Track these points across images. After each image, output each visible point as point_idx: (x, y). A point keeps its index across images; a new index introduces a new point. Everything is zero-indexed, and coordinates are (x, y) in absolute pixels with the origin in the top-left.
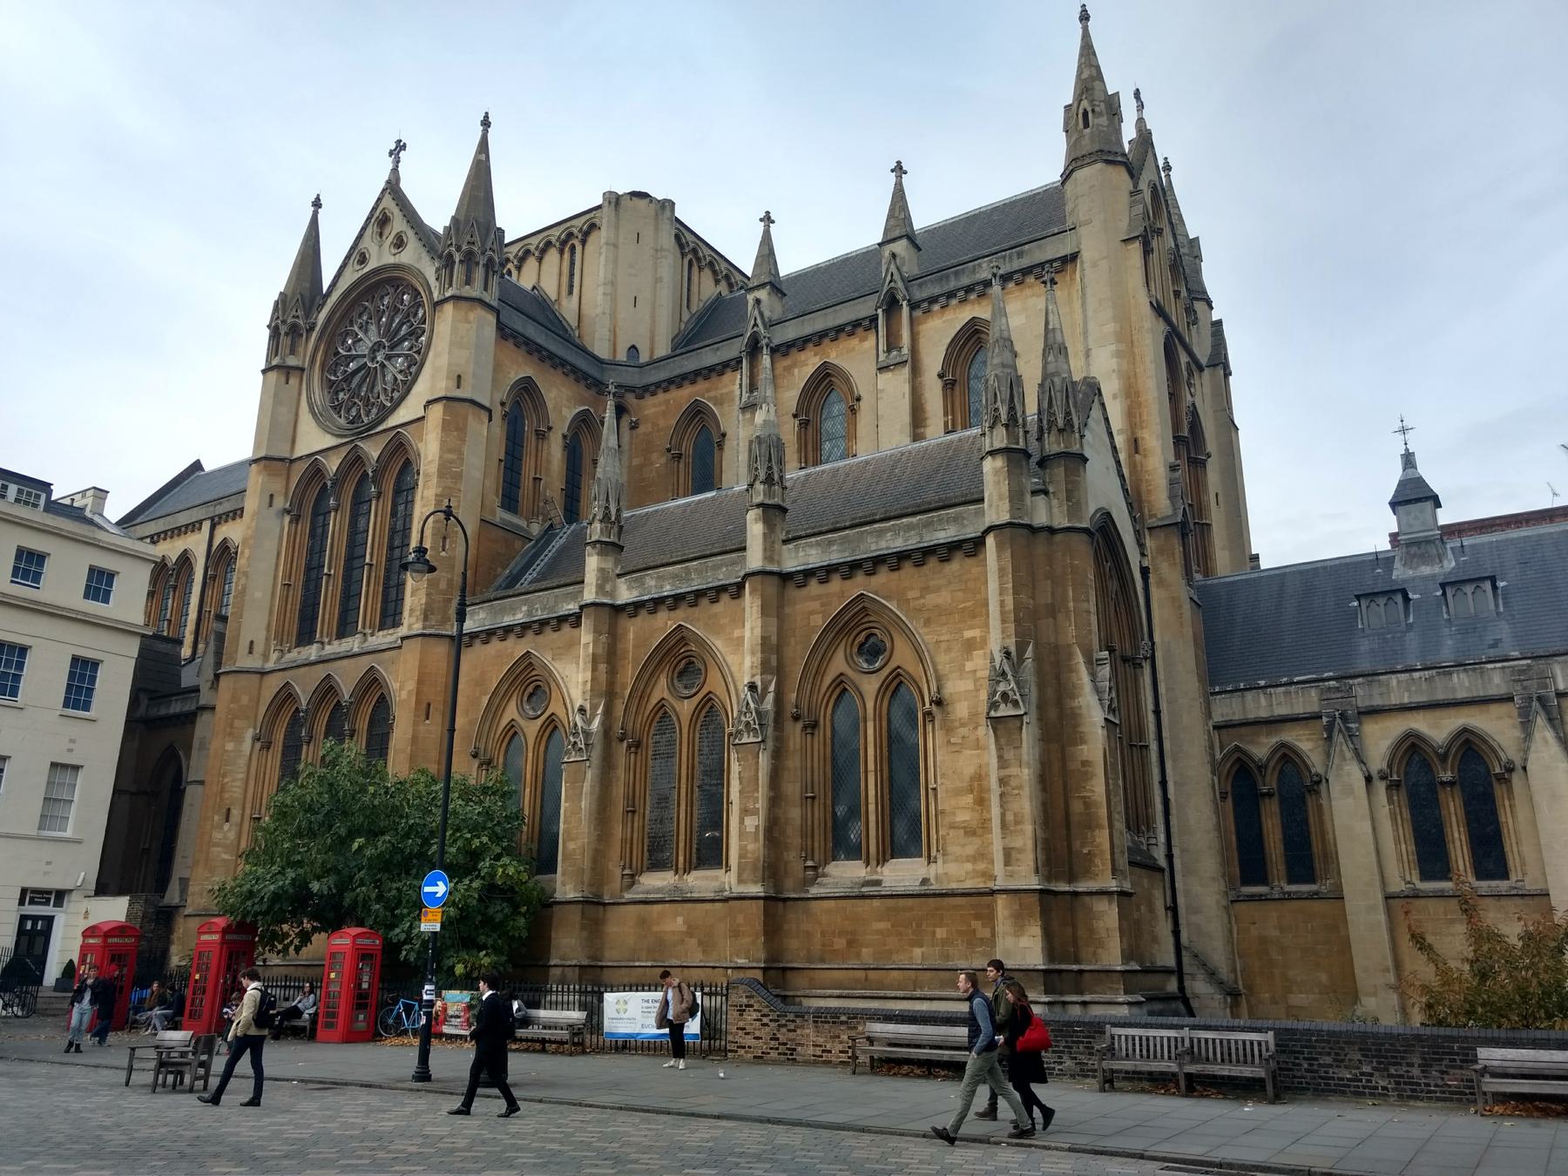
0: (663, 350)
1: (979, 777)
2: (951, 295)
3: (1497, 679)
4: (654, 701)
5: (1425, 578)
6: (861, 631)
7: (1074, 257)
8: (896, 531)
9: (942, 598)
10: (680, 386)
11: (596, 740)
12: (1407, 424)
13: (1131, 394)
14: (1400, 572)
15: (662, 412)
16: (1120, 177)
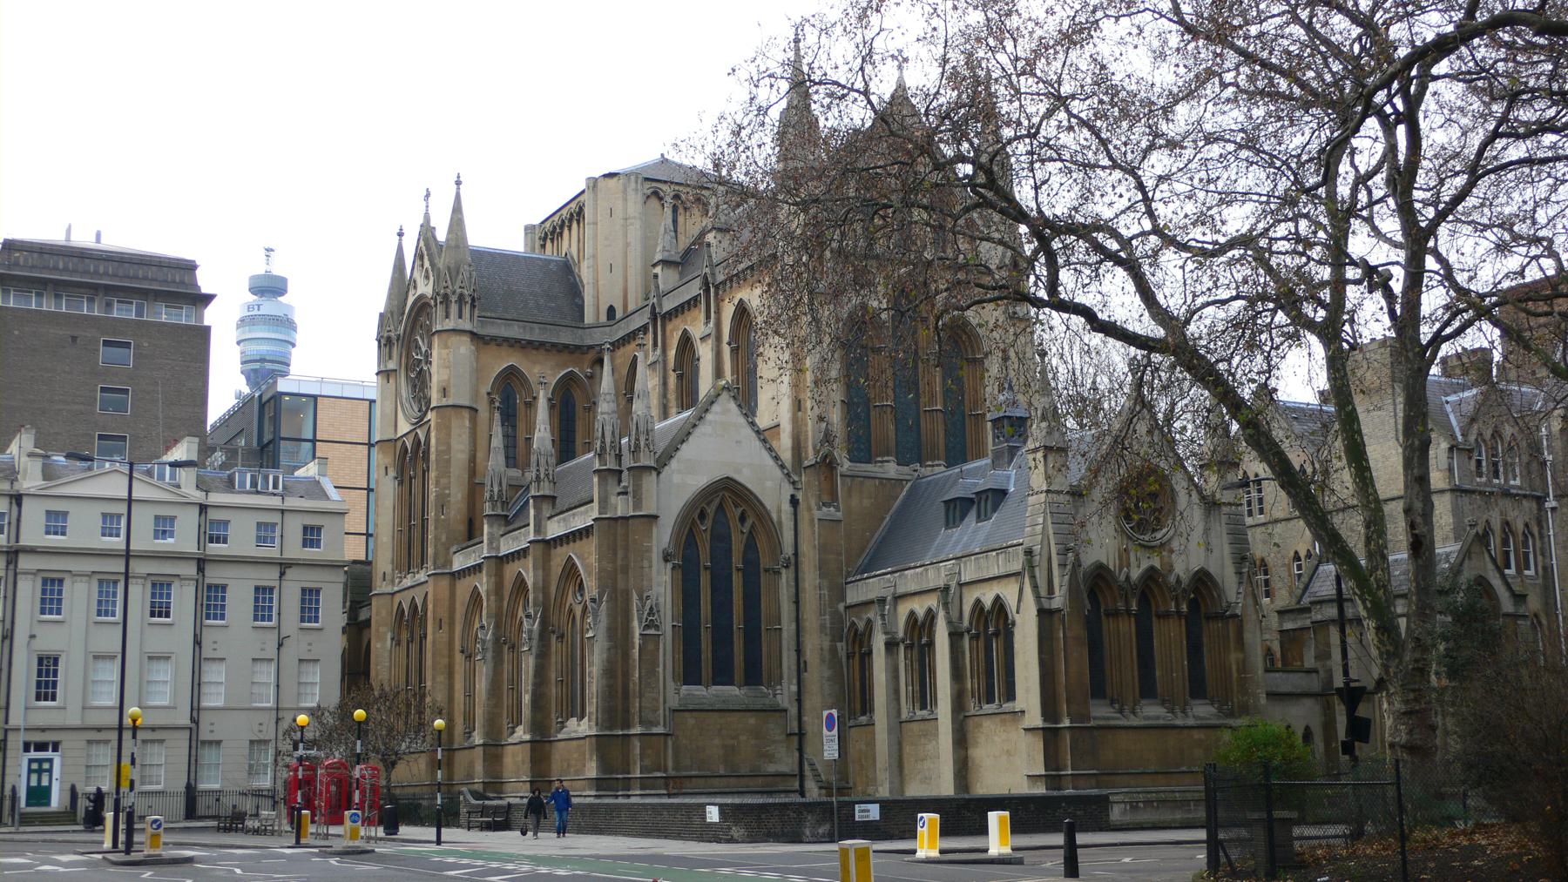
11: (489, 645)
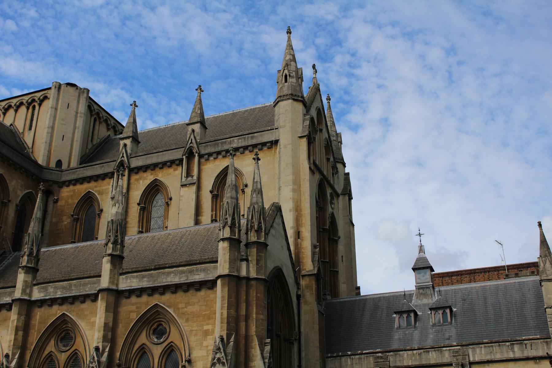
0: (74, 164)
2: (219, 153)
3: (447, 354)
4: (46, 352)
5: (425, 305)
6: (155, 322)
7: (276, 142)
8: (175, 273)
9: (195, 309)
10: (82, 183)
12: (421, 232)
13: (298, 210)
14: (414, 303)
15: (69, 196)
16: (300, 107)
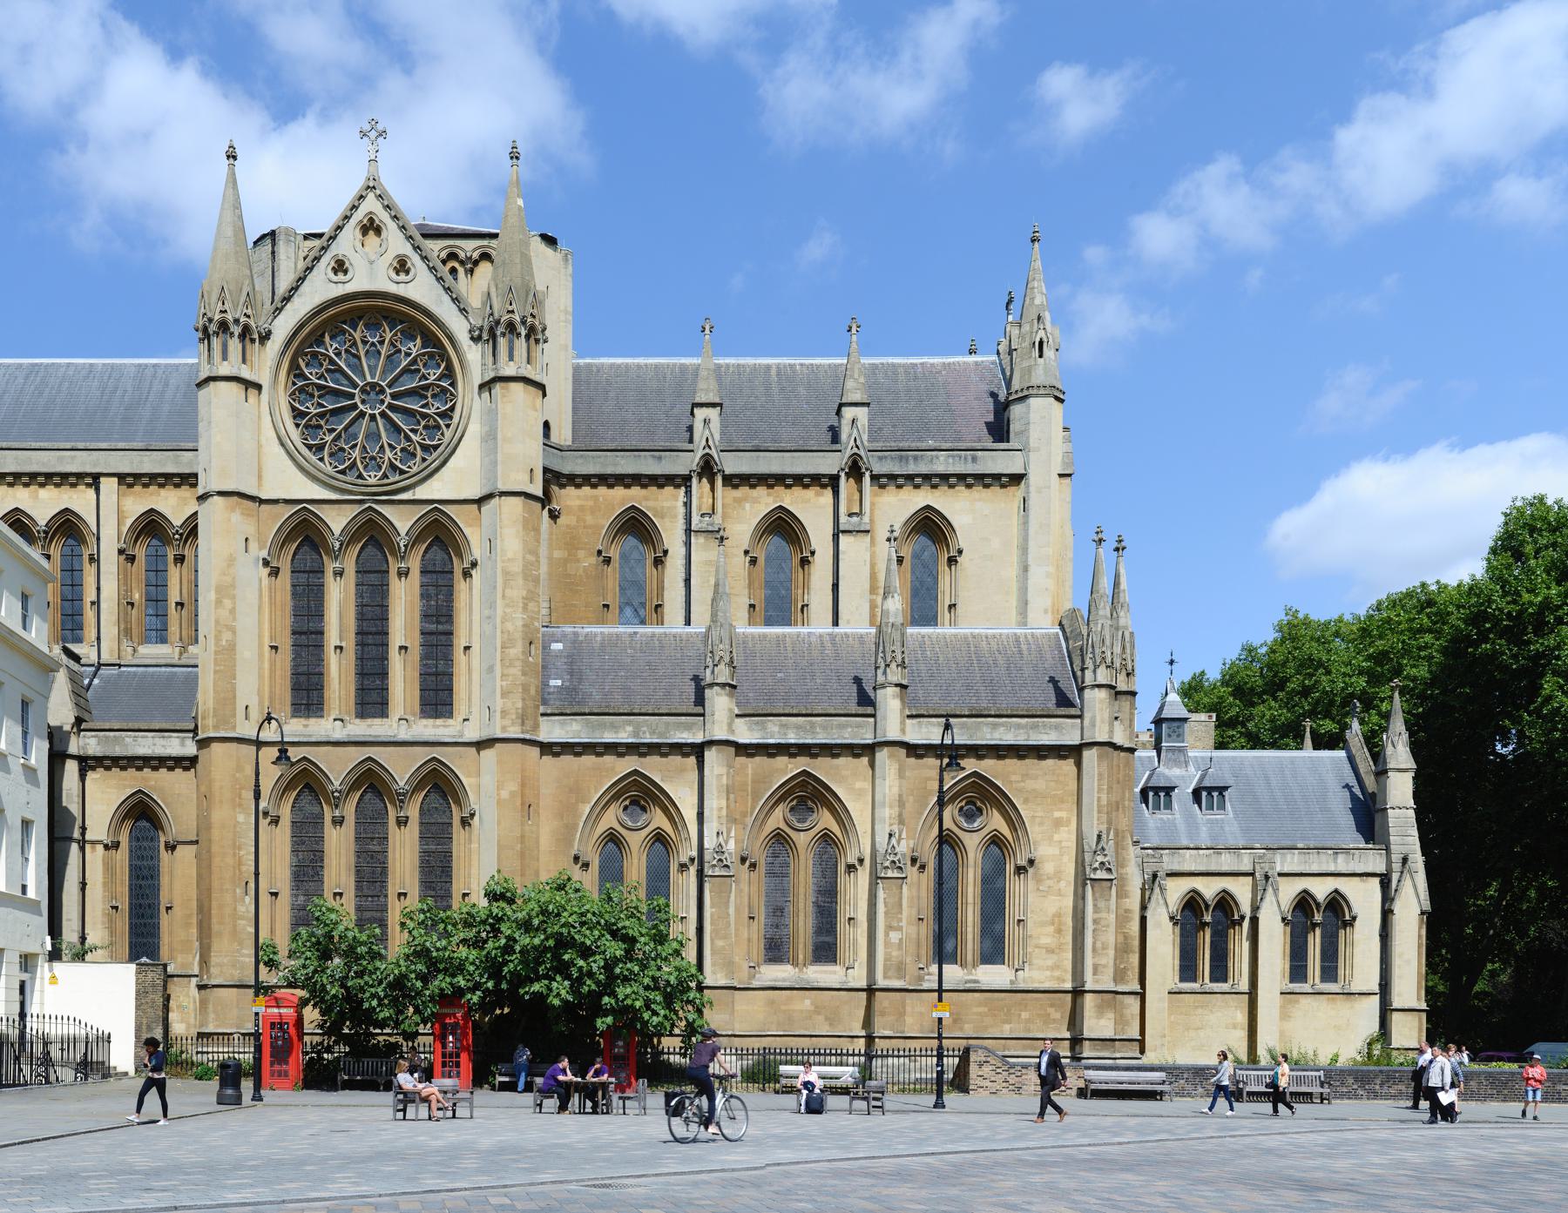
1: (1058, 915)
8: (1009, 727)
